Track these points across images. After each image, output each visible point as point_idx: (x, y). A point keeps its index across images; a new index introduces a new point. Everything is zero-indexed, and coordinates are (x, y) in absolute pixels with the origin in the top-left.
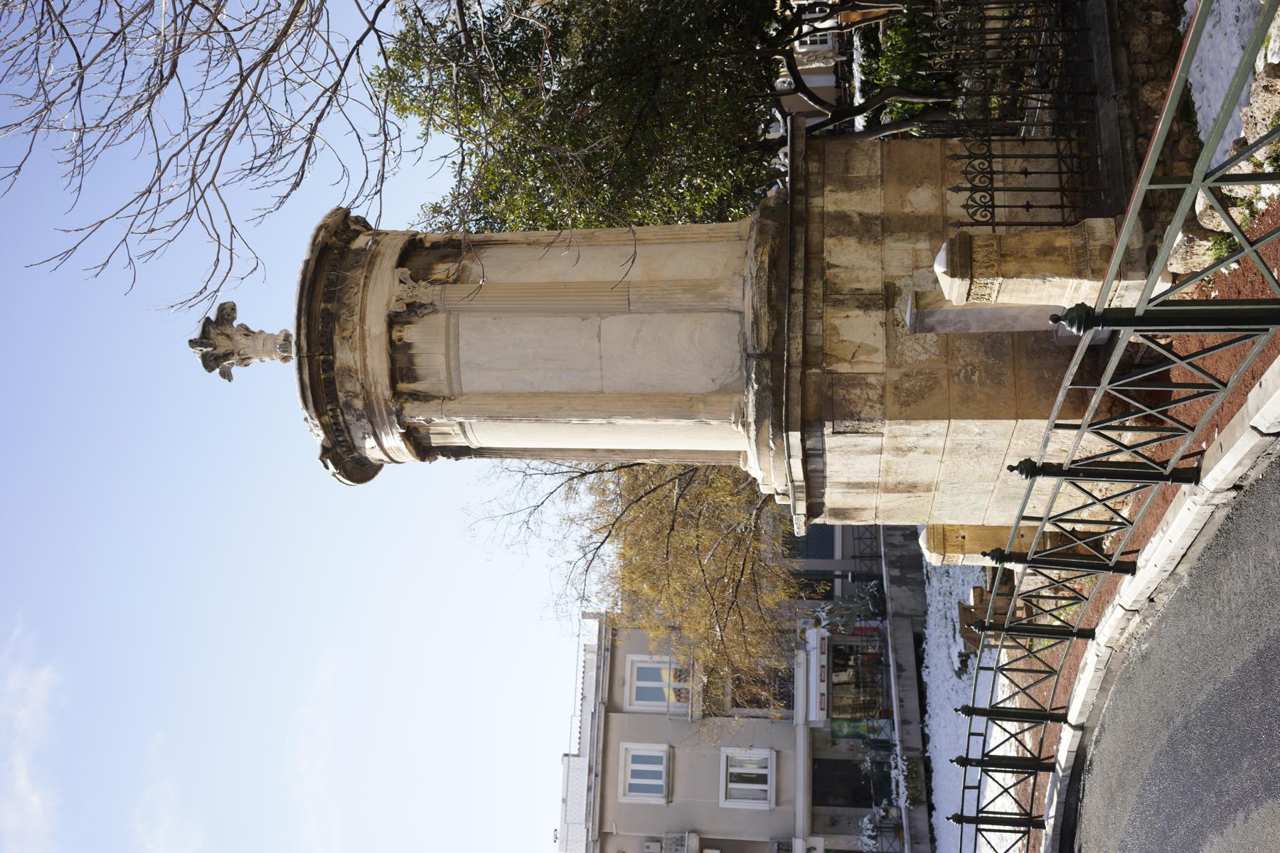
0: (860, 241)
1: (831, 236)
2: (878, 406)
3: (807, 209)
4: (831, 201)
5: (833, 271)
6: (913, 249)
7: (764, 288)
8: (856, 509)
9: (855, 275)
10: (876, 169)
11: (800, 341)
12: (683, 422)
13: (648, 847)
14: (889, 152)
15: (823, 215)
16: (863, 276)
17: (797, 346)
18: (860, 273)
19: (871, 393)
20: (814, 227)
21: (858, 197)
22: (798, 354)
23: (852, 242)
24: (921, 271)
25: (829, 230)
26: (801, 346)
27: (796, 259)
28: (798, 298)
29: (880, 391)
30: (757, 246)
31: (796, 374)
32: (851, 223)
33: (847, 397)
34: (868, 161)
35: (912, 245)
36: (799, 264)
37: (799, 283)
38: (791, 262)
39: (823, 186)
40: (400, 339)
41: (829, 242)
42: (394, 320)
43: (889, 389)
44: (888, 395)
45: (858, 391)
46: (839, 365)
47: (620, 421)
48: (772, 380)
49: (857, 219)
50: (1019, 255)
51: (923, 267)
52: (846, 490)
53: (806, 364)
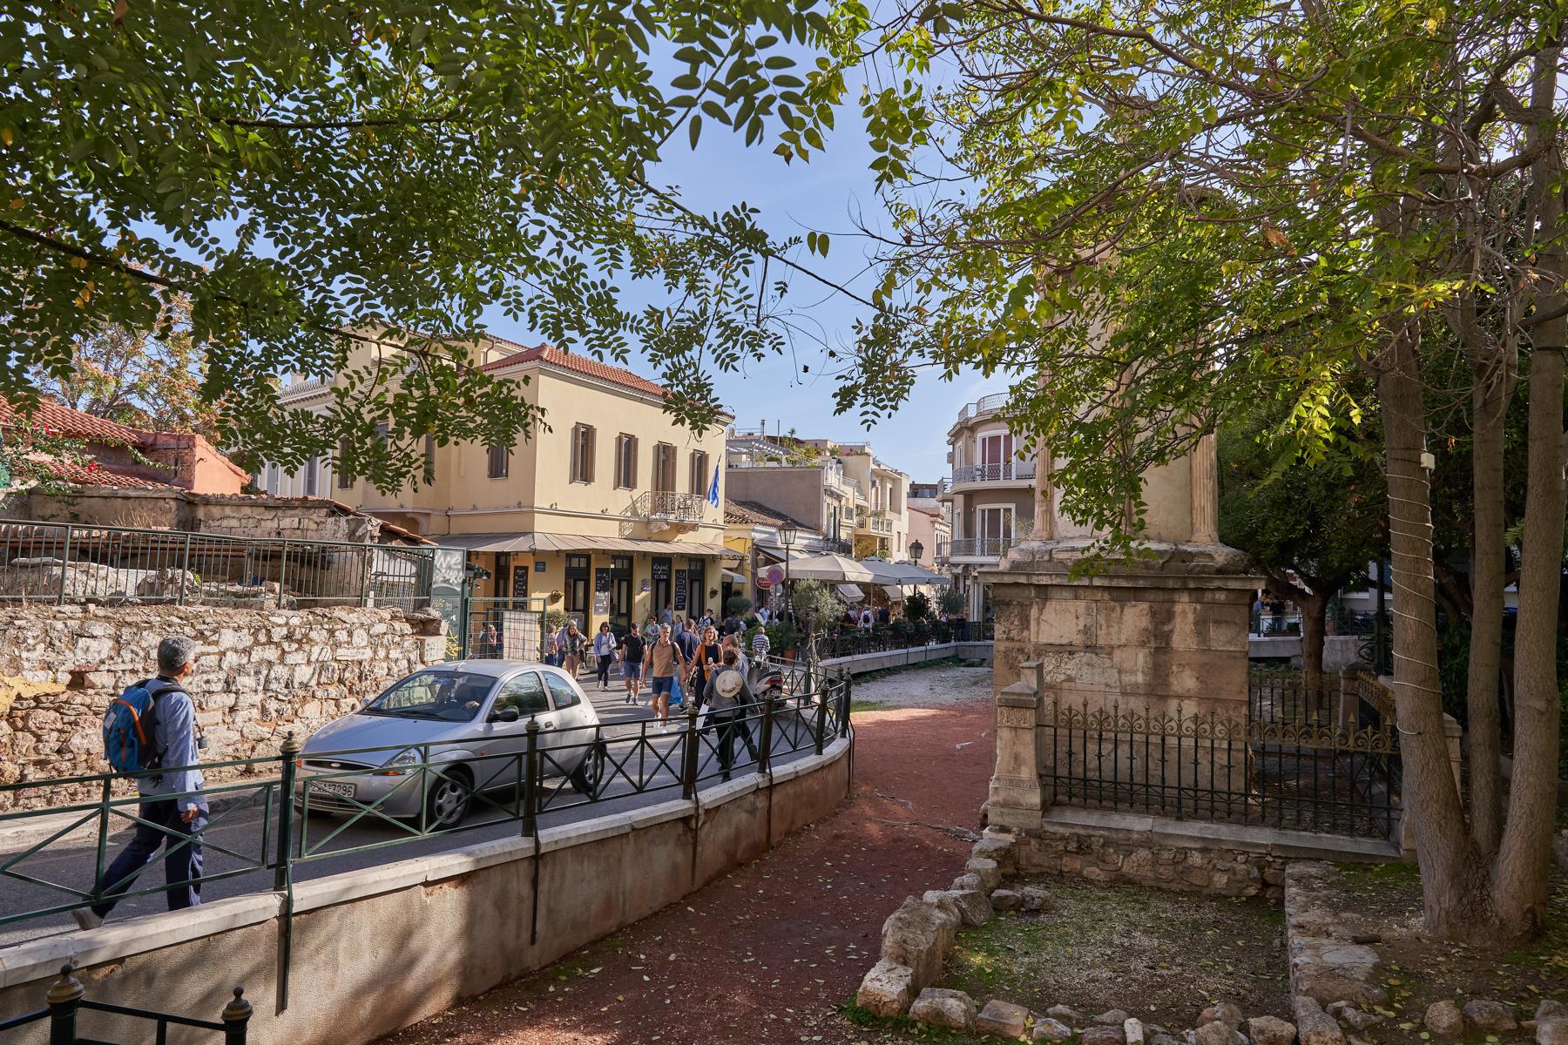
0: (1146, 630)
1: (1151, 607)
4: (1185, 611)
5: (1118, 609)
10: (1215, 646)
14: (1235, 658)
15: (1173, 602)
16: (1114, 630)
20: (1160, 596)
23: (1145, 622)
25: (1156, 606)
32: (1164, 624)
36: (1115, 583)
37: (1097, 582)
38: (1118, 577)
43: (1018, 645)
45: (1016, 623)
49: (1166, 628)
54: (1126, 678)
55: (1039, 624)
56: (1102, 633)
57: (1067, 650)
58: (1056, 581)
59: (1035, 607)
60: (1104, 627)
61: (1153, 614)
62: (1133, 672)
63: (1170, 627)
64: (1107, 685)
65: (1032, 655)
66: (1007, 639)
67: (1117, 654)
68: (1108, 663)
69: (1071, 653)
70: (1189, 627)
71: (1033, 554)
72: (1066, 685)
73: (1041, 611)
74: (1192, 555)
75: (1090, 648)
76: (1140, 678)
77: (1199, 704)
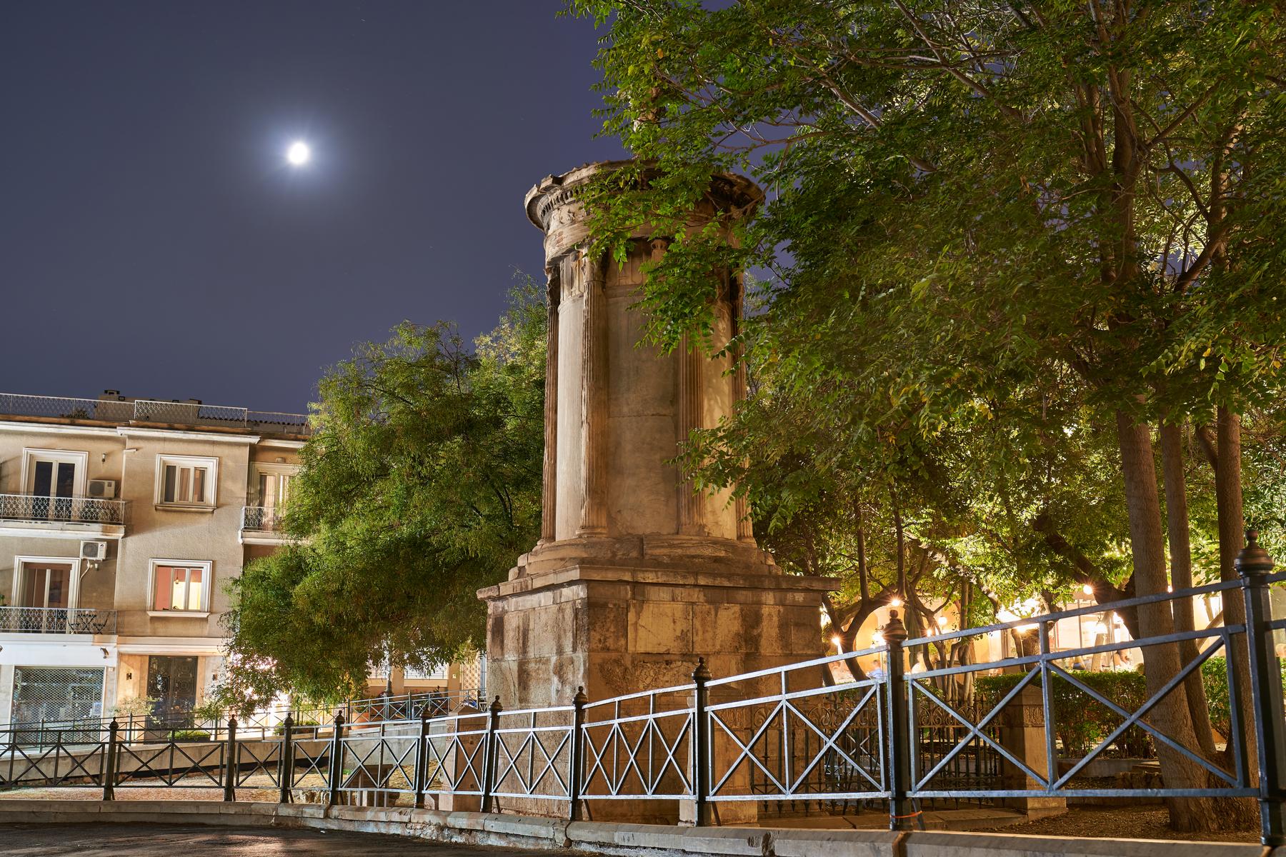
0: (738, 634)
1: (742, 610)
3: (765, 589)
5: (713, 612)
8: (502, 642)
9: (709, 629)
11: (655, 581)
12: (583, 486)
13: (110, 485)
16: (709, 635)
17: (650, 577)
23: (736, 626)
28: (691, 581)
31: (627, 577)
32: (753, 628)
36: (718, 582)
37: (702, 581)
38: (721, 576)
40: (654, 246)
41: (736, 608)
43: (614, 655)
45: (612, 629)
47: (584, 432)
49: (755, 632)
52: (521, 629)
53: (635, 584)
55: (636, 630)
56: (697, 639)
59: (632, 610)
60: (700, 633)
69: (668, 663)
70: (774, 632)
73: (638, 614)
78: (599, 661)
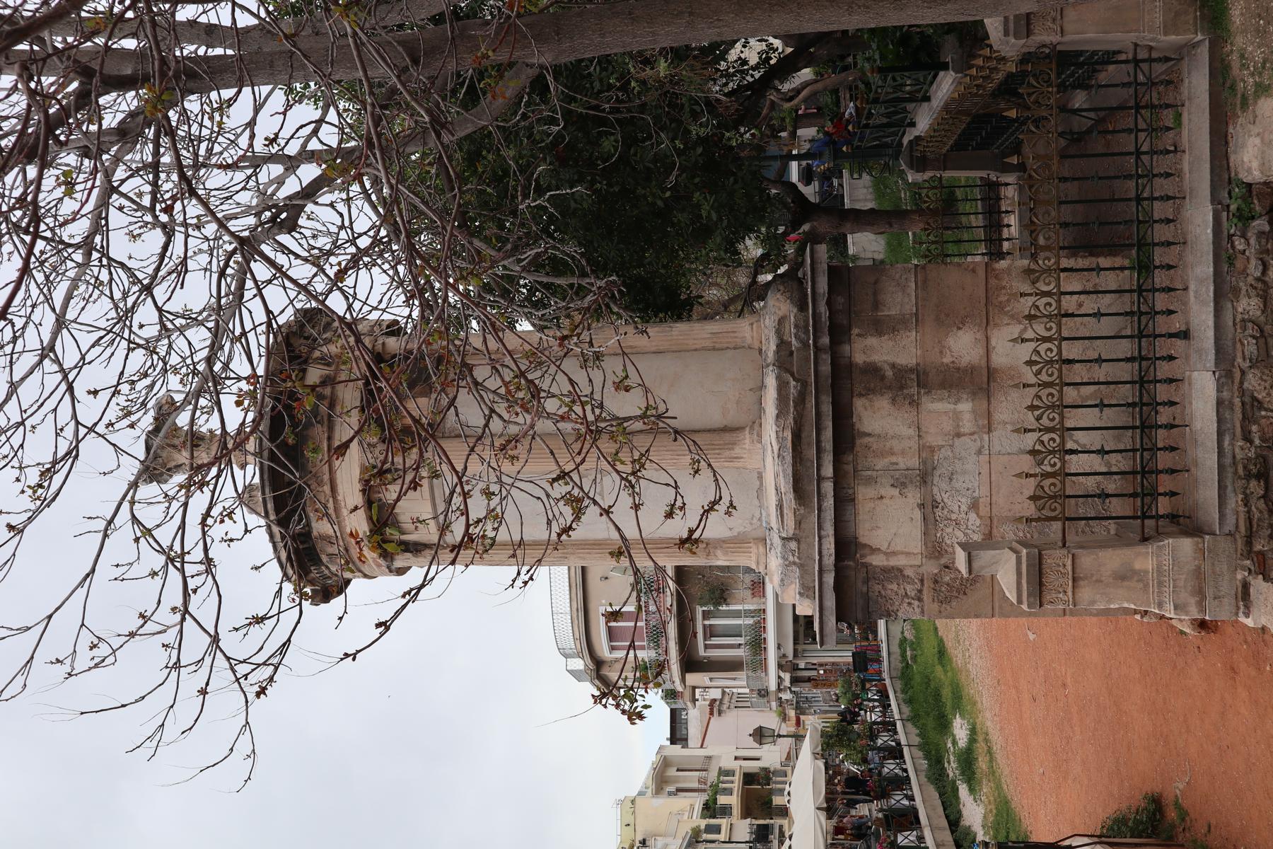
0: (894, 401)
1: (861, 395)
2: (916, 603)
6: (955, 412)
7: (790, 471)
9: (888, 445)
10: (910, 307)
14: (925, 281)
18: (894, 443)
19: (909, 588)
21: (891, 343)
22: (830, 555)
23: (883, 403)
24: (963, 438)
25: (858, 388)
26: (833, 546)
27: (823, 438)
29: (918, 586)
30: (778, 416)
32: (883, 378)
33: (883, 592)
34: (900, 294)
35: (952, 406)
36: (828, 445)
37: (828, 471)
38: (818, 442)
39: (850, 330)
42: (368, 490)
44: (925, 592)
45: (894, 587)
46: (874, 557)
48: (799, 558)
50: (1094, 579)
51: (964, 435)
54: (967, 425)
55: (894, 553)
56: (903, 463)
57: (930, 509)
58: (829, 529)
60: (894, 459)
61: (868, 392)
62: (957, 416)
63: (887, 367)
64: (979, 452)
65: (943, 561)
66: (920, 600)
67: (933, 439)
68: (946, 452)
69: (935, 505)
71: (787, 565)
72: (984, 511)
73: (875, 551)
74: (782, 344)
75: (925, 476)
76: (965, 407)
77: (996, 325)
78: (936, 605)
